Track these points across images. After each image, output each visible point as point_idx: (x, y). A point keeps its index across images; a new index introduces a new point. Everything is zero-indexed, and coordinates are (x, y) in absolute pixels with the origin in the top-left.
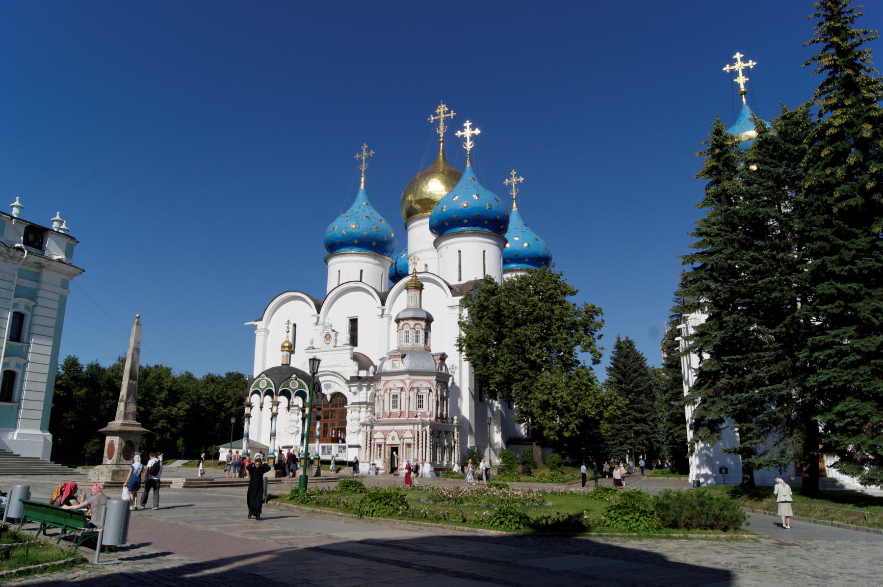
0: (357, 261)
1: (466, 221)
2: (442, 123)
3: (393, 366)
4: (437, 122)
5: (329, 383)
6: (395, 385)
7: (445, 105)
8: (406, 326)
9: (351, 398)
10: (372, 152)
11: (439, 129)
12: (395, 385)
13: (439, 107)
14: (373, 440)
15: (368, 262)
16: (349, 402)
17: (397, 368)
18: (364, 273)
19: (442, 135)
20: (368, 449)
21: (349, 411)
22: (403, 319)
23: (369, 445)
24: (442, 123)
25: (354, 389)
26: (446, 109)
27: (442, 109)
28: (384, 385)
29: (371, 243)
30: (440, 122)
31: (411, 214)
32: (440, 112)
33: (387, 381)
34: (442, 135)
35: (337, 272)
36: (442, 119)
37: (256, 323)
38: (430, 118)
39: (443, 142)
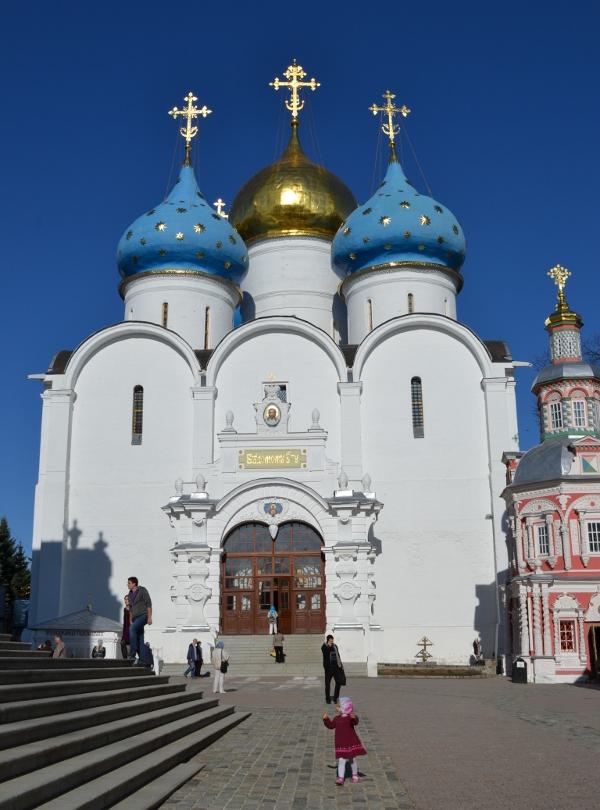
0: (201, 291)
1: (421, 248)
2: (295, 96)
3: (586, 466)
4: (286, 93)
5: (278, 501)
6: (593, 504)
7: (300, 68)
8: (578, 393)
9: (332, 531)
10: (205, 111)
11: (290, 103)
12: (593, 504)
13: (290, 68)
14: (555, 613)
15: (217, 296)
16: (329, 543)
17: (594, 471)
18: (209, 312)
19: (295, 114)
20: (548, 631)
21: (328, 556)
22: (571, 380)
23: (547, 625)
24: (295, 96)
25: (344, 514)
26: (303, 74)
27: (294, 72)
28: (568, 505)
29: (224, 263)
30: (292, 92)
31: (253, 231)
32: (292, 77)
33: (574, 497)
34: (295, 114)
35: (161, 309)
36: (295, 91)
37: (48, 378)
38: (274, 81)
39: (297, 124)
